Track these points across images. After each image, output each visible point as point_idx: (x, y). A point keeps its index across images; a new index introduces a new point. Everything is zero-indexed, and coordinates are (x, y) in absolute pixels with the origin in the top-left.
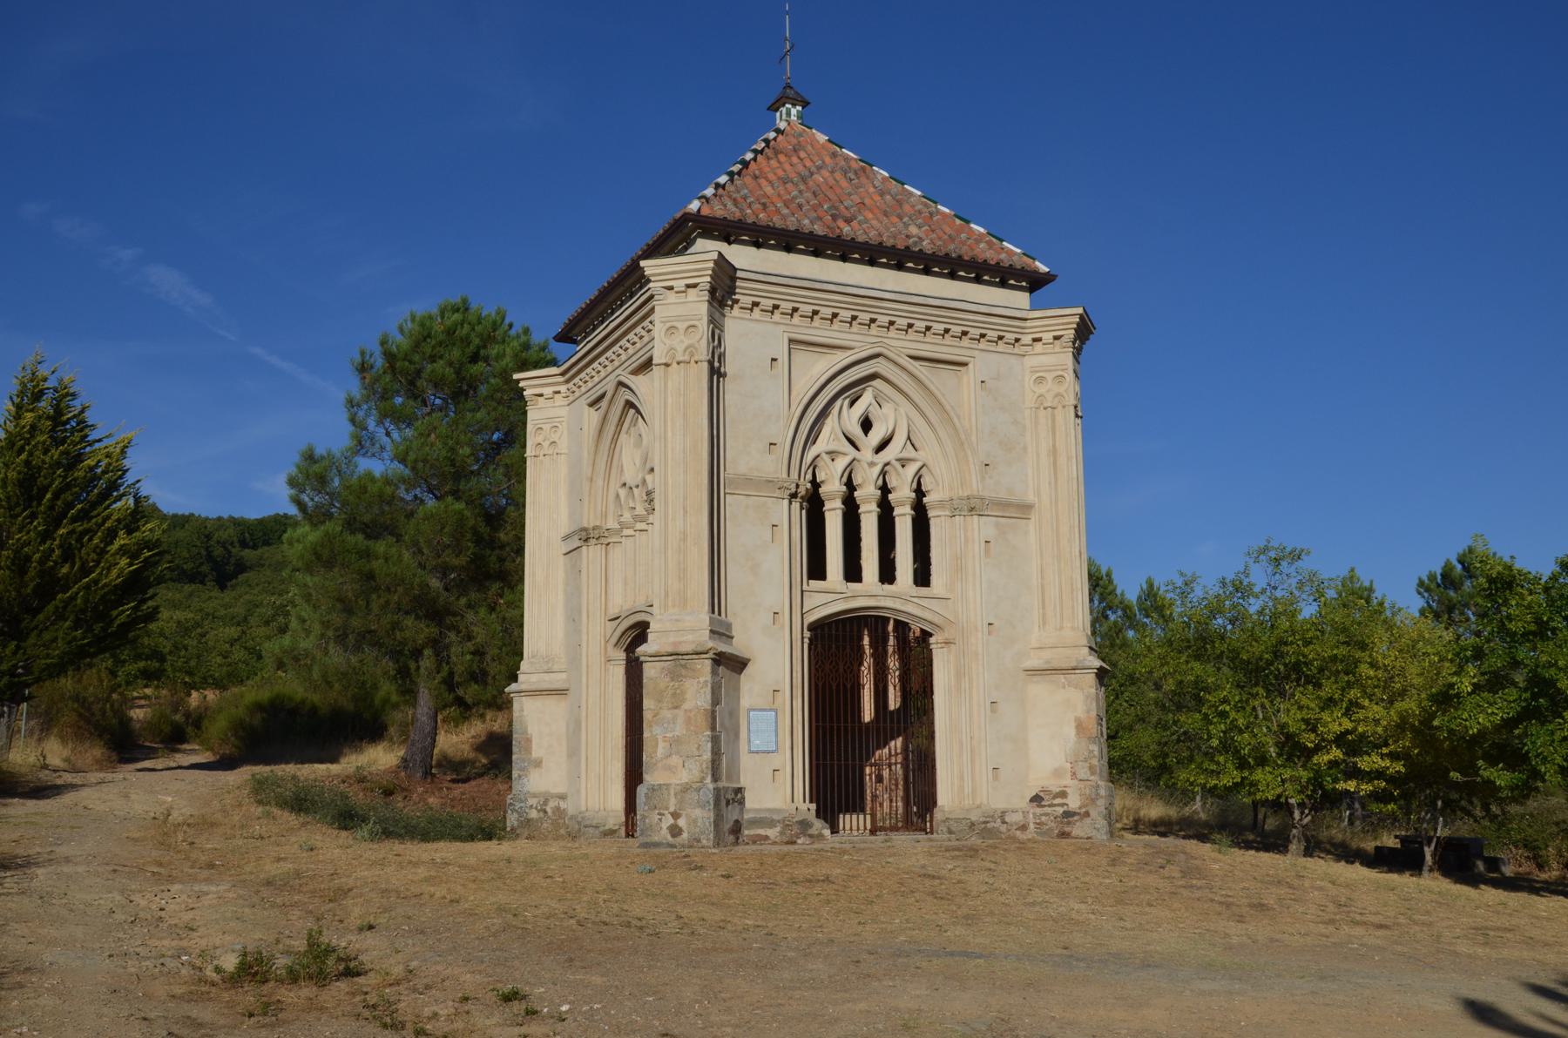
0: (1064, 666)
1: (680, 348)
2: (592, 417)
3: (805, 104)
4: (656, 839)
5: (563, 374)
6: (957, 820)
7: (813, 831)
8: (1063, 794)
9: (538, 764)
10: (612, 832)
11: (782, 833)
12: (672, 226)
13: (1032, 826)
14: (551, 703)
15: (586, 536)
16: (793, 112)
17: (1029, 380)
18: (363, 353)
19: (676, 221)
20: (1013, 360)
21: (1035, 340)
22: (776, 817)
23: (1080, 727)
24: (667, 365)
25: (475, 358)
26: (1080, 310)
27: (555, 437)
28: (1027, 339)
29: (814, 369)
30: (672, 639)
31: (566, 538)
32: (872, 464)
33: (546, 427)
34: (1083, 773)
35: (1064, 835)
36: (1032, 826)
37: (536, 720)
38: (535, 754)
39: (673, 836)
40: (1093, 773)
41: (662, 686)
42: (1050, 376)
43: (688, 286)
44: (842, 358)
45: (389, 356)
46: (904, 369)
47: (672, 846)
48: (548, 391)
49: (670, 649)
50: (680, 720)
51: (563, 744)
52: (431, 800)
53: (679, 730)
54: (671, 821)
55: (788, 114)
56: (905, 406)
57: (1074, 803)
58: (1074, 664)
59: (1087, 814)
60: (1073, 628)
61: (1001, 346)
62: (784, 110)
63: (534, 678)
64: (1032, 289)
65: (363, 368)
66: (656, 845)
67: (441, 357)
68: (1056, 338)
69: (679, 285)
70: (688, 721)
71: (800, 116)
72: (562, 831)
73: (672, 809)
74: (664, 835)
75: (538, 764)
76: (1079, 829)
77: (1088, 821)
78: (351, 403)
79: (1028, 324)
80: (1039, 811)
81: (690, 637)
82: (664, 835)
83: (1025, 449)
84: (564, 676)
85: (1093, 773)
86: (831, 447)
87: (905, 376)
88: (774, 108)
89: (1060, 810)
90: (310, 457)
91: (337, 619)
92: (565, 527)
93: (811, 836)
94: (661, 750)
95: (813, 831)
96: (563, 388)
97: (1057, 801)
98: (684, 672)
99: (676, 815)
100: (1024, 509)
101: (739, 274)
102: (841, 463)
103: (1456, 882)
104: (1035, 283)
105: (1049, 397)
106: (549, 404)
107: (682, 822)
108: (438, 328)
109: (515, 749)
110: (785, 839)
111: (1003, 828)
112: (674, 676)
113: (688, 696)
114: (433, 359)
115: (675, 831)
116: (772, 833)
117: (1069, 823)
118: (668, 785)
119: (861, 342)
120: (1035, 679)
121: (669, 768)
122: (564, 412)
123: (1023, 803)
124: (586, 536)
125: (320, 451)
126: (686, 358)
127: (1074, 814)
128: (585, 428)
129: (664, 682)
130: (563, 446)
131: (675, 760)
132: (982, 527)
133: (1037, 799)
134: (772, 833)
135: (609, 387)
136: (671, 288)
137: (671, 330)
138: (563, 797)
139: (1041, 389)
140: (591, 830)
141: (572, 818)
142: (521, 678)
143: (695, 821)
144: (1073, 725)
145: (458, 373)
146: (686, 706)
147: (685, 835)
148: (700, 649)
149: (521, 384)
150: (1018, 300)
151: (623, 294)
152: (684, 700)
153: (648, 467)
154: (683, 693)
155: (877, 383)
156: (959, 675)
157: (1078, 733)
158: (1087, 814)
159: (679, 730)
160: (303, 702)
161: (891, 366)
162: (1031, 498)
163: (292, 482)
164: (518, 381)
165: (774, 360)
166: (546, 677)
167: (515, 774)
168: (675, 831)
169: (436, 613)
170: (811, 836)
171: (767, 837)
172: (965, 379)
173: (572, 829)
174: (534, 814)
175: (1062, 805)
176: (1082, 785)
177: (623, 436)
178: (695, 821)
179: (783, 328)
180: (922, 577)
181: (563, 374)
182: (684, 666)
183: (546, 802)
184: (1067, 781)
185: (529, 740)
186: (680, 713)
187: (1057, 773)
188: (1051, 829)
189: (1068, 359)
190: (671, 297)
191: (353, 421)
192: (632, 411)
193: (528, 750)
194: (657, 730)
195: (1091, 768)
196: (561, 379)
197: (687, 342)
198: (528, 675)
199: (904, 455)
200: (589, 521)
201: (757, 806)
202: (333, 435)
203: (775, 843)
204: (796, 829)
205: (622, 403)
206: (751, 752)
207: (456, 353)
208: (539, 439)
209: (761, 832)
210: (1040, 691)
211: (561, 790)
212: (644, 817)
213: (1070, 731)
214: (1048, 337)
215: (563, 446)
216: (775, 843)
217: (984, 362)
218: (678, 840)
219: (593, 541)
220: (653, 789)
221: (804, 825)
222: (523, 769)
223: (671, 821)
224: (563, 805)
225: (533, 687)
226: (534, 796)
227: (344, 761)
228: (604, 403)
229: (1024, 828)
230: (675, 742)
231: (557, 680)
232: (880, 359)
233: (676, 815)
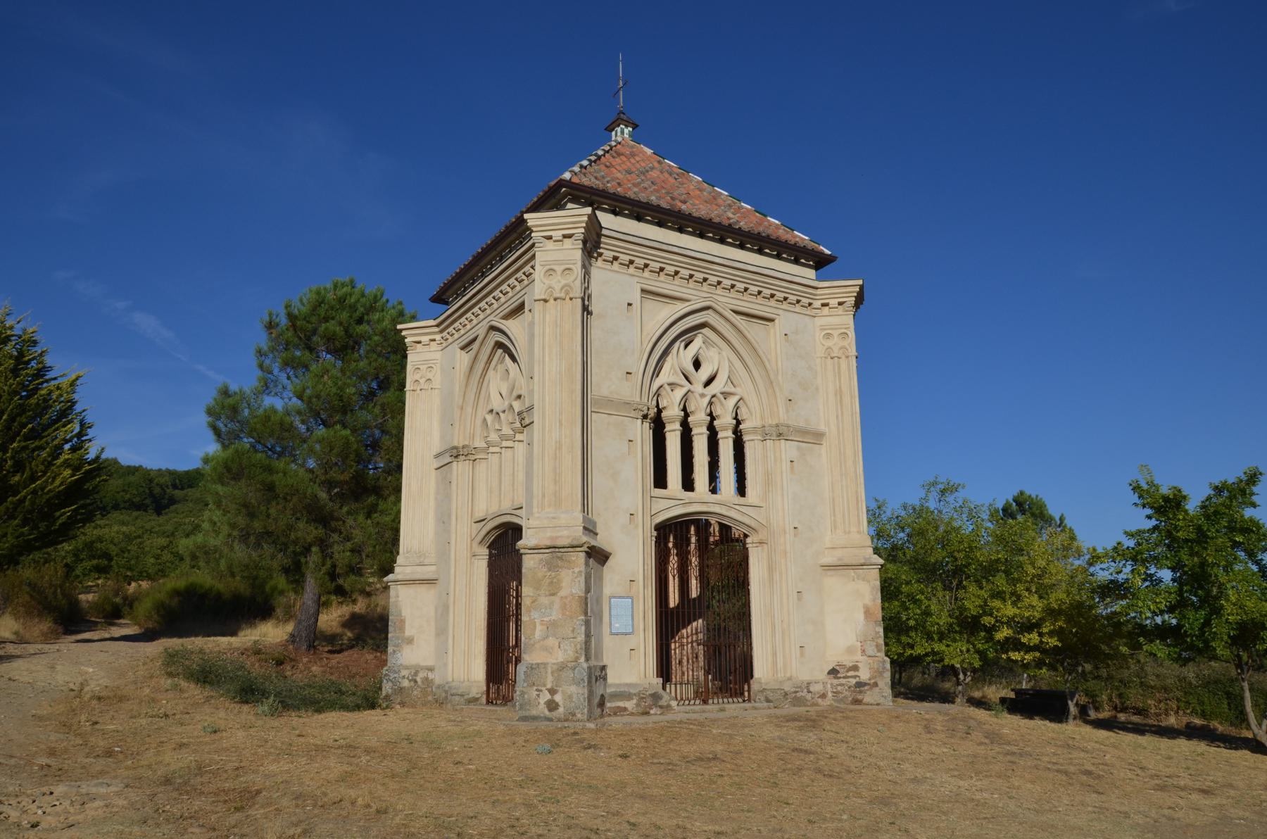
1: (557, 287)
2: (464, 359)
3: (635, 126)
4: (534, 712)
5: (437, 326)
6: (773, 691)
8: (855, 668)
9: (410, 641)
10: (475, 700)
11: (638, 705)
13: (830, 694)
14: (422, 590)
15: (456, 453)
16: (626, 131)
17: (819, 335)
18: (270, 315)
19: (550, 188)
21: (823, 305)
23: (868, 612)
24: (546, 301)
25: (360, 321)
26: (860, 282)
27: (430, 376)
28: (817, 304)
29: (665, 313)
30: (548, 534)
31: (437, 456)
32: (702, 395)
33: (423, 367)
34: (871, 650)
35: (857, 702)
36: (830, 694)
37: (409, 605)
38: (408, 633)
39: (550, 710)
40: (879, 651)
41: (540, 575)
42: (836, 333)
43: (565, 236)
44: (681, 308)
45: (291, 316)
47: (550, 720)
48: (425, 339)
49: (549, 543)
50: (556, 606)
51: (434, 623)
52: (314, 668)
53: (555, 615)
54: (548, 696)
55: (622, 132)
56: (727, 351)
57: (864, 675)
58: (862, 561)
59: (876, 685)
60: (859, 532)
61: (798, 308)
62: (619, 129)
63: (408, 570)
65: (270, 326)
66: (535, 718)
67: (333, 318)
68: (840, 304)
69: (557, 235)
70: (564, 607)
72: (430, 698)
73: (549, 686)
74: (542, 709)
75: (410, 641)
76: (868, 697)
77: (876, 690)
78: (260, 353)
79: (819, 292)
80: (835, 682)
81: (565, 533)
82: (542, 709)
83: (817, 389)
84: (433, 568)
86: (672, 380)
87: (728, 326)
88: (610, 129)
89: (853, 681)
90: (225, 393)
91: (241, 521)
92: (437, 447)
93: (661, 707)
94: (538, 633)
96: (438, 337)
97: (851, 673)
99: (552, 692)
100: (816, 437)
101: (604, 232)
102: (679, 393)
103: (1051, 721)
104: (820, 262)
105: (836, 350)
106: (426, 349)
107: (558, 698)
108: (330, 296)
109: (390, 629)
110: (641, 710)
111: (809, 697)
112: (551, 566)
114: (326, 319)
115: (552, 706)
116: (630, 705)
117: (861, 692)
118: (545, 664)
119: (697, 296)
121: (546, 649)
122: (438, 355)
123: (822, 676)
124: (456, 453)
125: (234, 387)
126: (562, 295)
127: (866, 684)
128: (457, 367)
129: (542, 572)
130: (437, 382)
131: (552, 641)
132: (788, 449)
133: (833, 672)
134: (630, 705)
135: (481, 330)
136: (550, 238)
137: (550, 272)
138: (431, 669)
139: (829, 343)
140: (457, 698)
141: (438, 687)
142: (397, 569)
143: (570, 697)
144: (862, 611)
145: (346, 331)
146: (562, 593)
147: (561, 710)
148: (575, 543)
149: (404, 333)
151: (494, 258)
152: (560, 588)
153: (515, 394)
154: (559, 581)
155: (706, 331)
156: (771, 569)
158: (876, 685)
159: (555, 615)
160: (211, 589)
161: (717, 317)
162: (822, 428)
163: (210, 412)
164: (401, 330)
165: (630, 305)
166: (419, 569)
167: (390, 649)
168: (552, 706)
169: (322, 518)
170: (661, 707)
171: (625, 709)
173: (441, 698)
174: (406, 683)
175: (855, 677)
177: (491, 372)
178: (570, 697)
179: (636, 279)
180: (741, 490)
181: (437, 326)
182: (561, 558)
183: (416, 674)
184: (858, 657)
185: (403, 621)
186: (556, 599)
187: (850, 650)
189: (849, 320)
190: (550, 245)
191: (261, 367)
192: (500, 351)
193: (402, 629)
194: (535, 615)
195: (877, 646)
196: (437, 329)
197: (563, 282)
198: (403, 568)
199: (727, 389)
200: (459, 441)
201: (617, 682)
202: (245, 380)
203: (632, 714)
204: (649, 701)
205: (492, 343)
206: (612, 634)
207: (344, 316)
208: (417, 377)
209: (621, 704)
210: (833, 583)
211: (430, 663)
212: (523, 693)
213: (860, 616)
214: (833, 302)
215: (437, 382)
216: (632, 714)
217: (787, 320)
218: (555, 714)
219: (462, 458)
220: (532, 667)
221: (656, 697)
222: (397, 646)
223: (548, 696)
224: (431, 676)
225: (408, 578)
226: (407, 668)
227: (241, 634)
228: (476, 346)
229: (823, 696)
230: (552, 626)
231: (428, 572)
232: (710, 312)
233: (552, 692)
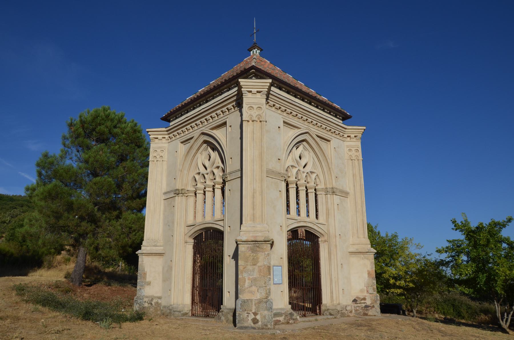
0: (364, 251)
1: (254, 115)
2: (182, 149)
3: (261, 50)
4: (246, 325)
5: (167, 131)
6: (333, 310)
7: (294, 317)
8: (364, 299)
9: (149, 284)
10: (186, 314)
11: (285, 319)
12: (242, 71)
13: (353, 311)
14: (156, 259)
15: (178, 193)
16: (258, 52)
17: (346, 150)
18: (71, 120)
19: (245, 69)
20: (342, 142)
21: (348, 136)
22: (283, 312)
23: (369, 274)
24: (248, 121)
25: (115, 127)
26: (365, 128)
27: (161, 154)
28: (346, 136)
29: (294, 132)
30: (251, 235)
31: (165, 193)
32: (303, 172)
33: (159, 150)
34: (371, 291)
35: (366, 314)
36: (353, 311)
37: (149, 265)
38: (148, 280)
39: (254, 323)
40: (374, 291)
41: (248, 255)
42: (353, 149)
43: (258, 92)
44: (299, 132)
45: (83, 122)
46: (314, 139)
47: (254, 328)
48: (160, 137)
49: (253, 239)
50: (256, 271)
51: (165, 274)
52: (85, 295)
53: (256, 275)
54: (253, 316)
55: (256, 52)
56: (312, 154)
57: (368, 302)
58: (367, 251)
59: (373, 306)
60: (364, 237)
61: (338, 137)
62: (255, 51)
63: (148, 248)
64: (343, 119)
65: (71, 125)
66: (246, 328)
67: (103, 124)
68: (355, 136)
69: (254, 91)
70: (260, 271)
71: (260, 54)
72: (159, 312)
73: (253, 311)
74: (250, 323)
75: (149, 284)
76: (371, 312)
77: (374, 309)
78: (65, 138)
79: (347, 130)
80: (356, 305)
81: (260, 234)
82: (250, 323)
83: (346, 173)
84: (162, 248)
85: (374, 291)
86: (292, 164)
87: (314, 142)
88: (250, 50)
89: (364, 305)
90: (46, 156)
91: (52, 220)
92: (165, 189)
93: (294, 319)
94: (247, 284)
95: (294, 317)
96: (167, 136)
97: (363, 301)
98: (258, 249)
99: (255, 314)
100: (345, 194)
101: (271, 92)
102: (295, 171)
104: (345, 118)
105: (353, 156)
106: (160, 141)
107: (258, 317)
108: (102, 114)
109: (139, 277)
110: (286, 321)
111: (346, 312)
112: (253, 251)
113: (260, 260)
114: (100, 124)
115: (255, 321)
116: (281, 319)
117: (367, 310)
118: (251, 300)
119: (304, 127)
120: (354, 255)
121: (251, 292)
122: (166, 145)
123: (350, 302)
124: (178, 193)
125: (51, 154)
126: (256, 119)
127: (369, 306)
128: (179, 151)
129: (249, 253)
130: (165, 158)
131: (254, 288)
132: (336, 199)
133: (355, 301)
134: (281, 319)
135: (196, 134)
136: (250, 92)
137: (251, 108)
138: (160, 298)
139: (350, 153)
140: (177, 313)
141: (165, 307)
142: (143, 248)
143: (265, 317)
144: (367, 273)
145: (110, 130)
146: (259, 264)
147: (260, 323)
148: (266, 239)
149: (149, 133)
150: (340, 122)
151: (203, 101)
152: (258, 262)
153: (215, 166)
154: (258, 258)
155: (304, 143)
156: (330, 253)
157: (369, 276)
158: (373, 306)
159: (256, 275)
160: (8, 252)
161: (310, 137)
162: (348, 190)
163: (38, 165)
164: (148, 132)
165: (279, 127)
166: (154, 248)
167: (138, 287)
168: (255, 321)
169: (93, 220)
170: (294, 319)
171: (280, 321)
172: (329, 146)
173: (168, 313)
174: (146, 305)
175: (364, 303)
176: (371, 295)
177: (198, 155)
178: (265, 317)
179: (281, 116)
180: (317, 217)
181: (167, 131)
182: (258, 247)
183: (152, 300)
184: (365, 294)
185: (145, 274)
186: (256, 267)
187: (362, 291)
188: (360, 312)
189: (359, 144)
190: (250, 95)
191: (64, 145)
192: (205, 145)
193: (145, 278)
194: (245, 275)
195: (374, 289)
196: (166, 133)
197: (257, 113)
198: (145, 247)
199: (312, 170)
200: (179, 186)
201: (276, 307)
202: (56, 150)
203: (283, 323)
204: (289, 316)
205: (202, 141)
206: (274, 284)
207: (109, 123)
208: (155, 154)
209: (278, 318)
210: (354, 259)
211: (159, 295)
212: (240, 315)
213: (366, 275)
214: (352, 136)
215: (165, 158)
216: (283, 323)
217: (335, 142)
218: (257, 325)
219: (180, 195)
220: (244, 302)
221: (291, 314)
222: (142, 286)
223: (253, 316)
224: (160, 301)
225: (149, 252)
226: (147, 297)
227: (30, 274)
228: (192, 141)
229: (351, 312)
230: (254, 281)
231: (160, 250)
232: (307, 134)
233: (255, 314)
